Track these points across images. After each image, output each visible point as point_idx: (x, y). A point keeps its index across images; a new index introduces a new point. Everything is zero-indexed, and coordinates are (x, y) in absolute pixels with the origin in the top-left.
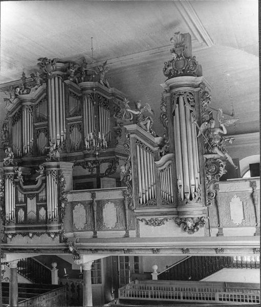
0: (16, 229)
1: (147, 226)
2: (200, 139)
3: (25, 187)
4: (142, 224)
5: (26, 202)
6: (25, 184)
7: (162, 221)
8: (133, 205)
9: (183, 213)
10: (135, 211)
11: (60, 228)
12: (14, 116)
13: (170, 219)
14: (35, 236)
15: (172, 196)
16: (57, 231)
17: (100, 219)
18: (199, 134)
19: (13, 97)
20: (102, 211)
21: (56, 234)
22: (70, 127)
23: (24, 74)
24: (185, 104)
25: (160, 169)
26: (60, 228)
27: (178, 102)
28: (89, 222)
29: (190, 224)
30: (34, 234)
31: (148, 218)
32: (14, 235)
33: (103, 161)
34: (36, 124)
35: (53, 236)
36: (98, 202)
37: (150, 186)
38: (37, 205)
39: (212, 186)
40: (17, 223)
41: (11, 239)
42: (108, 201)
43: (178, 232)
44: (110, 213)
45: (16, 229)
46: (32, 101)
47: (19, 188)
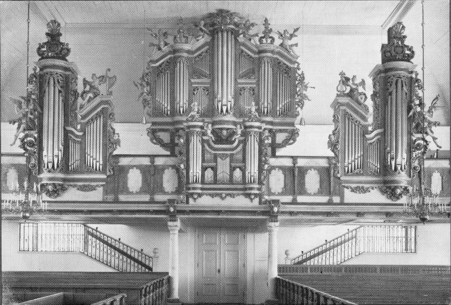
0: (202, 189)
2: (410, 120)
3: (216, 146)
4: (347, 192)
6: (215, 142)
7: (368, 188)
8: (338, 173)
9: (393, 182)
11: (259, 189)
12: (160, 66)
13: (373, 189)
14: (228, 198)
16: (257, 192)
17: (302, 184)
19: (162, 43)
20: (304, 177)
21: (256, 195)
24: (402, 86)
25: (369, 142)
26: (259, 189)
28: (288, 187)
29: (399, 191)
30: (227, 195)
31: (353, 186)
32: (200, 195)
33: (281, 131)
34: (192, 81)
35: (253, 197)
36: (299, 168)
38: (230, 166)
39: (417, 162)
40: (203, 182)
41: (195, 199)
42: (310, 168)
43: (383, 199)
44: (312, 181)
45: (202, 189)
46: (188, 52)
47: (207, 147)
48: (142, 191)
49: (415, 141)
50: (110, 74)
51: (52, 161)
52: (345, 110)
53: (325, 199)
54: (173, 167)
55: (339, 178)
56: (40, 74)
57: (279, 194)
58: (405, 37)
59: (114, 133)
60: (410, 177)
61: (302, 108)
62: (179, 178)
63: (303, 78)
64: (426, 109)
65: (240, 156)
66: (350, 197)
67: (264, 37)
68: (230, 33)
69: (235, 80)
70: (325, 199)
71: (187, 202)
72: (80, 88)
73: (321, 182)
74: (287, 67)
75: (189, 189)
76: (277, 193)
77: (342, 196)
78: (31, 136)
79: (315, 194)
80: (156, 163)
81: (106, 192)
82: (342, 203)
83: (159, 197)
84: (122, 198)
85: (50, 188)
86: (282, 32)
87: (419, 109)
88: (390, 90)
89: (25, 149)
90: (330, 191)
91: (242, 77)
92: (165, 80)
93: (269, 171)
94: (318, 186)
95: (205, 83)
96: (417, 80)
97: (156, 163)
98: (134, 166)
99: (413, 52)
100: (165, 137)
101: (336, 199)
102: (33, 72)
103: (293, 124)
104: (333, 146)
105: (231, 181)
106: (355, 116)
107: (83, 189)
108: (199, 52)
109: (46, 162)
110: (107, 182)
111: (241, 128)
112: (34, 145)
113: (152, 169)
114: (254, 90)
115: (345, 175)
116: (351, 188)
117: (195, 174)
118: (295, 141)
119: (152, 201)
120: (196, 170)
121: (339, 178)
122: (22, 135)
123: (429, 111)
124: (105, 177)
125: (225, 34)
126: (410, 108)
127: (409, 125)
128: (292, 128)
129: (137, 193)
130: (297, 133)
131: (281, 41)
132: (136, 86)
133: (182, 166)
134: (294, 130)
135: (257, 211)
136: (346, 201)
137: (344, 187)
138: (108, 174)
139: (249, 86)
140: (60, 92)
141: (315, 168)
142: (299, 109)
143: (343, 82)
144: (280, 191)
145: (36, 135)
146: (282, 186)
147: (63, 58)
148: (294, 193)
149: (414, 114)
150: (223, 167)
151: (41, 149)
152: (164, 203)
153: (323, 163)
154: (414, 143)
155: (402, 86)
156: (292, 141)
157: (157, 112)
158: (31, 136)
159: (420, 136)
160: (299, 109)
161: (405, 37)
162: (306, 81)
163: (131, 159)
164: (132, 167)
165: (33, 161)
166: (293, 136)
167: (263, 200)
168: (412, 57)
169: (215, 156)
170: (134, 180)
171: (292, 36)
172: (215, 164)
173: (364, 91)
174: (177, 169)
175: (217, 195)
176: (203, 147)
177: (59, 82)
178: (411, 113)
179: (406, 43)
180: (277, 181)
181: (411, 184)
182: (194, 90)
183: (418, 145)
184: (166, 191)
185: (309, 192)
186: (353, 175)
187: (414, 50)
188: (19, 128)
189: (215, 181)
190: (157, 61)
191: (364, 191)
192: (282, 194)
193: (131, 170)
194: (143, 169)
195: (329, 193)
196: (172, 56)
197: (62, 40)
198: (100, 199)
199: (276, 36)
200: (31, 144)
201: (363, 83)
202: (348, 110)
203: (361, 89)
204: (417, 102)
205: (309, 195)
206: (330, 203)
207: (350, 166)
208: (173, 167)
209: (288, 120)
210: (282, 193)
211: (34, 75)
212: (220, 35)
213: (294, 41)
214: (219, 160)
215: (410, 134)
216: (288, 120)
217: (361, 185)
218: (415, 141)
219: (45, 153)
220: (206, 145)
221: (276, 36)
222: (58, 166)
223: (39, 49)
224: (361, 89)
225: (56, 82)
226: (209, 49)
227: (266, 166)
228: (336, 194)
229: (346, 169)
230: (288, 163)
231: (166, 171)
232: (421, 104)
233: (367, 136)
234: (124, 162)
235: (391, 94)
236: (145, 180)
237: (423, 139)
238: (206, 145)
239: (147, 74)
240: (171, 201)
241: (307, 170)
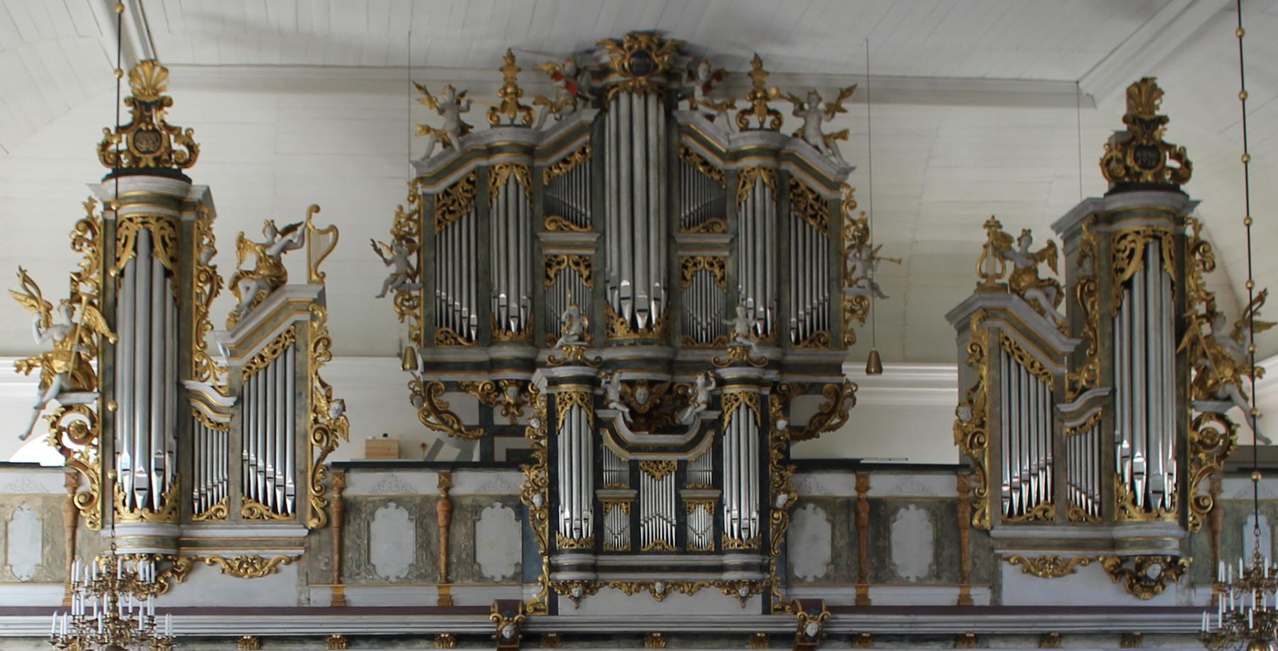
1: (1028, 576)
4: (1009, 573)
5: (635, 483)
10: (993, 533)
12: (446, 193)
15: (1097, 497)
18: (1182, 346)
20: (888, 530)
22: (685, 267)
23: (511, 56)
24: (1162, 260)
27: (1145, 257)
33: (806, 389)
36: (876, 503)
37: (1042, 462)
44: (912, 540)
48: (419, 575)
49: (1198, 421)
50: (319, 222)
51: (146, 485)
52: (999, 330)
53: (947, 595)
54: (506, 500)
55: (987, 532)
56: (105, 221)
57: (818, 582)
58: (1163, 120)
59: (329, 398)
60: (1186, 528)
61: (862, 320)
62: (525, 537)
63: (865, 231)
64: (1226, 330)
65: (704, 473)
66: (1019, 587)
67: (751, 111)
68: (652, 100)
69: (670, 237)
70: (947, 595)
71: (553, 609)
72: (226, 263)
73: (938, 543)
74: (818, 198)
75: (554, 568)
76: (810, 579)
77: (994, 584)
78: (80, 407)
79: (920, 582)
80: (457, 490)
81: (307, 580)
82: (996, 608)
83: (465, 594)
84: (355, 596)
85: (142, 569)
86: (802, 95)
87: (1206, 329)
88: (1126, 276)
89: (64, 450)
90: (962, 572)
91: (691, 224)
92: (463, 232)
93: (790, 510)
94: (927, 556)
95: (585, 246)
96: (1199, 244)
97: (457, 490)
98: (391, 499)
99: (1187, 165)
100: (465, 407)
101: (981, 596)
102: (84, 214)
103: (836, 369)
104: (969, 436)
105: (682, 542)
106: (1028, 347)
107: (241, 568)
108: (564, 153)
109: (127, 489)
110: (307, 549)
111: (707, 383)
112: (89, 435)
113: (440, 508)
114: (722, 267)
115: (1004, 523)
116: (1020, 560)
117: (576, 524)
118: (844, 418)
119: (447, 607)
120: (572, 515)
121: (987, 532)
122: (54, 406)
123: (1236, 335)
124: (306, 532)
125: (638, 102)
126: (1181, 327)
127: (1182, 381)
128: (837, 379)
129: (401, 582)
130: (852, 395)
131: (799, 122)
132: (379, 252)
133: (537, 500)
134: (841, 385)
135: (754, 634)
136: (1007, 600)
137: (1000, 556)
138: (313, 523)
139: (709, 254)
140: (167, 273)
141: (920, 503)
142: (854, 324)
143: (996, 249)
144: (821, 572)
145: (94, 406)
146: (825, 552)
147: (178, 175)
148: (860, 579)
149: (1195, 341)
150: (658, 502)
151: (109, 452)
152: (485, 610)
153: (944, 487)
154: (1196, 428)
155: (1162, 260)
156: (836, 421)
157: (438, 328)
158: (80, 407)
159: (1211, 406)
160: (854, 324)
161: (1163, 120)
162: (875, 239)
163: (379, 476)
164: (386, 501)
165: (87, 486)
166: (838, 404)
167: (775, 604)
168: (1185, 179)
169: (634, 467)
170: (392, 541)
171: (834, 109)
172: (633, 493)
173: (1053, 276)
174: (521, 511)
175: (647, 585)
176: (597, 440)
177: (165, 245)
178: (1185, 340)
179: (1169, 135)
180: (814, 544)
181: (1187, 546)
182: (549, 265)
183: (1212, 433)
184: (487, 574)
185: (903, 574)
186: (1027, 523)
187: (1190, 156)
188: (44, 386)
189: (635, 546)
190: (438, 177)
191: (1062, 569)
192: (828, 580)
193: (380, 512)
194: (420, 510)
195: (962, 579)
196: (483, 162)
197: (171, 116)
198: (292, 602)
199: (786, 108)
200: (83, 434)
201: (1049, 253)
202: (1009, 331)
203: (1044, 271)
204: (1201, 308)
205: (905, 583)
206: (964, 607)
207: (1015, 496)
208: (506, 500)
209: (823, 355)
210: (827, 577)
211: (89, 224)
212: (624, 99)
213: (837, 123)
214: (645, 479)
215: (1183, 402)
216: (823, 355)
217: (1050, 554)
218: (1198, 421)
219: (123, 460)
220: (606, 434)
221: (786, 108)
222: (162, 502)
223: (105, 145)
224: (1044, 271)
225: (158, 247)
226: (591, 143)
227: (782, 499)
228: (980, 582)
229: (1007, 504)
230: (839, 485)
231: (486, 513)
232: (1211, 315)
233: (1064, 408)
234: (361, 485)
235: (1128, 284)
236: (424, 542)
237: (1221, 418)
238: (606, 434)
239: (409, 218)
240: (508, 608)
241: (896, 510)
